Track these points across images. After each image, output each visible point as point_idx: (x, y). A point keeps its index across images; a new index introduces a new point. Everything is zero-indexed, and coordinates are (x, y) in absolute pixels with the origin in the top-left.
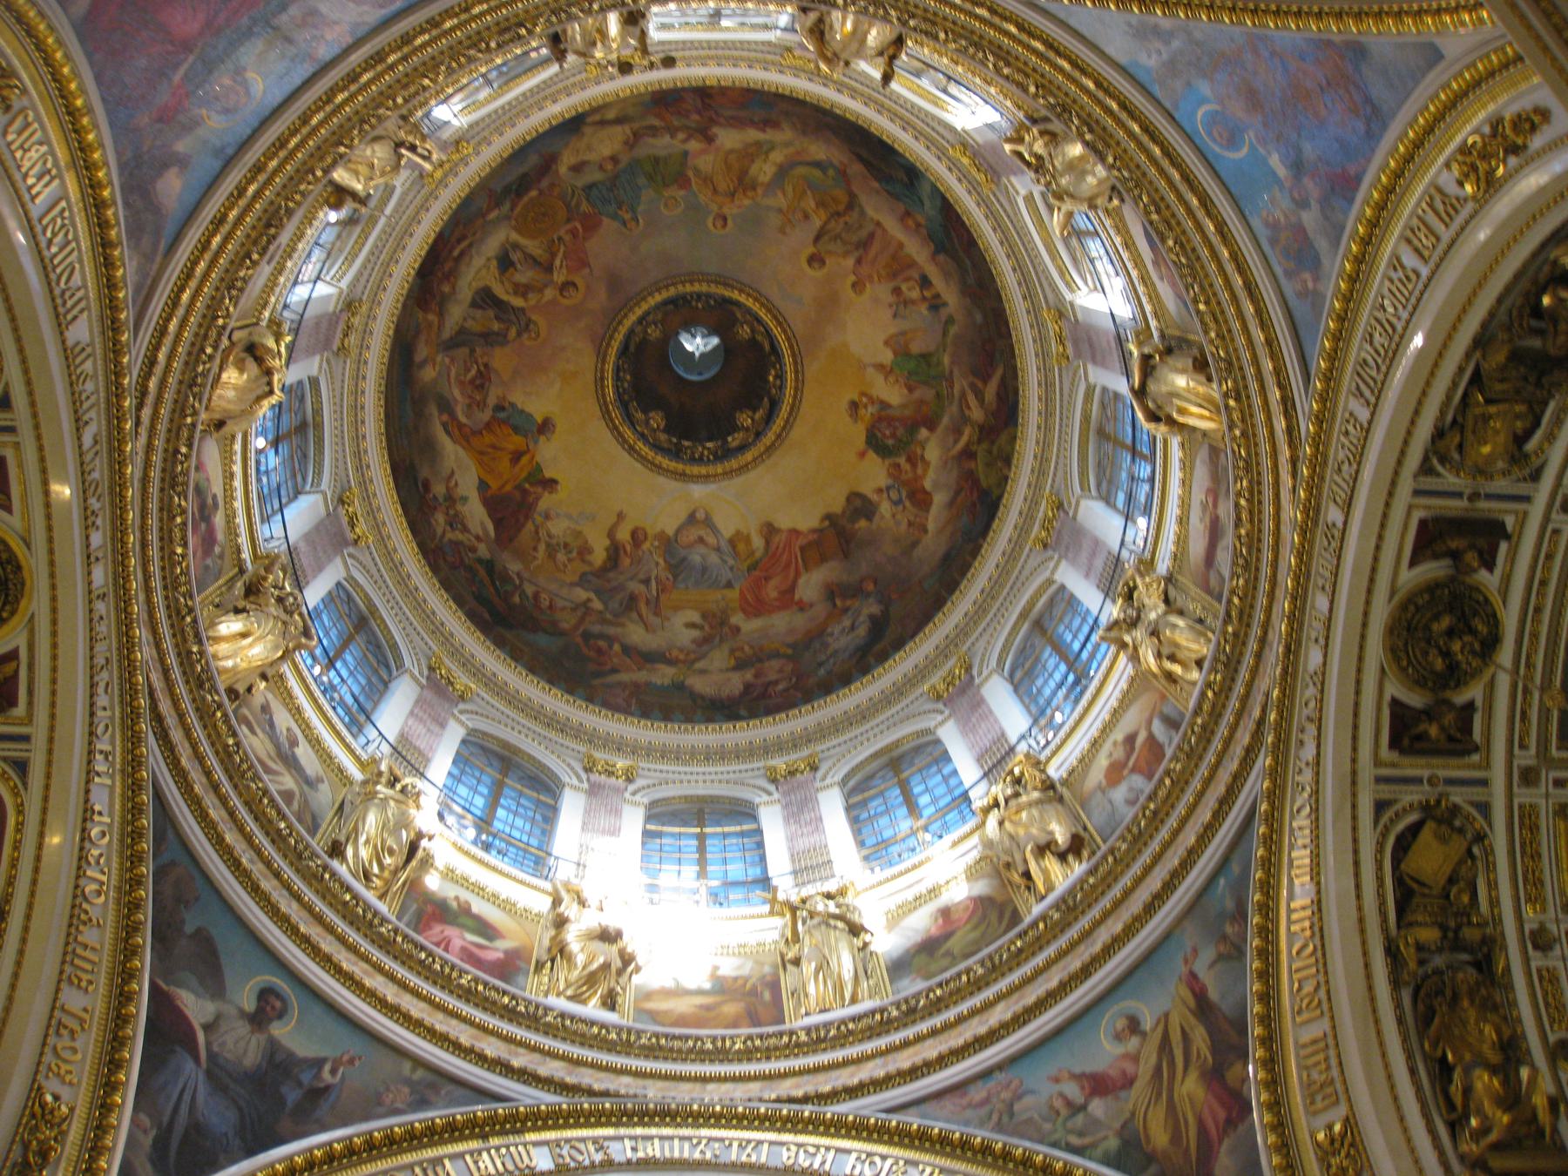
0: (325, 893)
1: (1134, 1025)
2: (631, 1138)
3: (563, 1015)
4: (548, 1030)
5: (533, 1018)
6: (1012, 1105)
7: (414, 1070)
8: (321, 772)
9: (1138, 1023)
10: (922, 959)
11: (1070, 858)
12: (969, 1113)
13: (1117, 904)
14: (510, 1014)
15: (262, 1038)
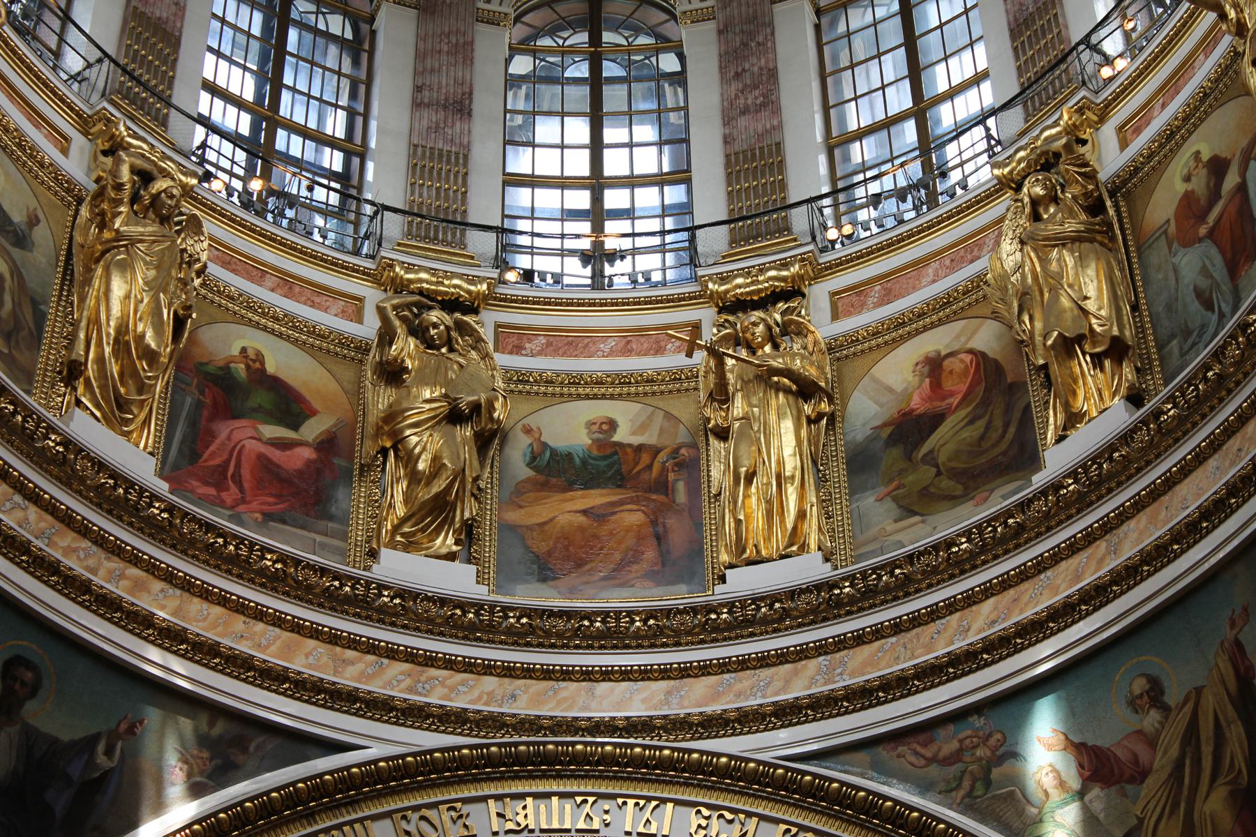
0: (69, 480)
1: (1155, 694)
2: (499, 798)
3: (402, 593)
4: (385, 617)
5: (364, 601)
6: (990, 771)
7: (211, 724)
8: (33, 203)
9: (1162, 693)
10: (896, 452)
11: (1107, 363)
12: (934, 771)
13: (1155, 494)
14: (332, 601)
15: (14, 730)
